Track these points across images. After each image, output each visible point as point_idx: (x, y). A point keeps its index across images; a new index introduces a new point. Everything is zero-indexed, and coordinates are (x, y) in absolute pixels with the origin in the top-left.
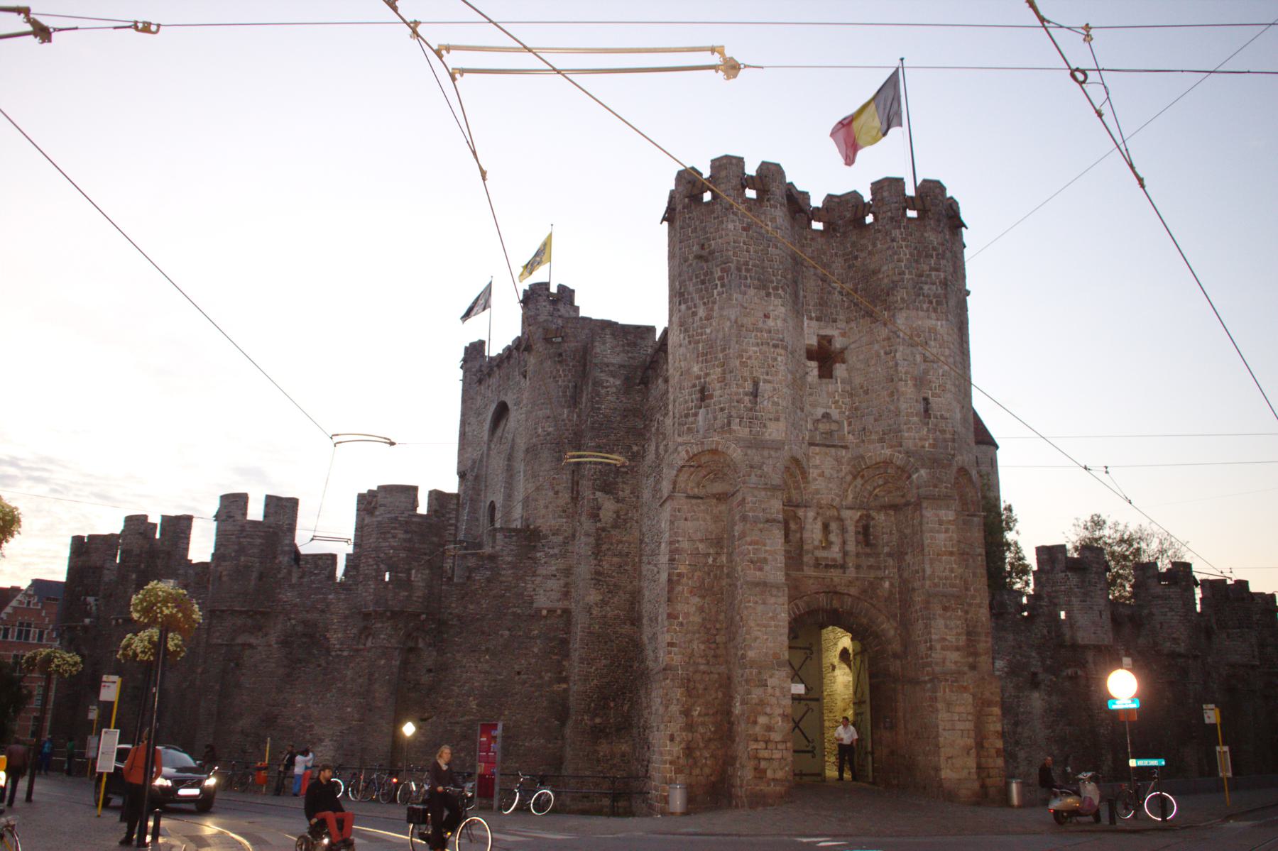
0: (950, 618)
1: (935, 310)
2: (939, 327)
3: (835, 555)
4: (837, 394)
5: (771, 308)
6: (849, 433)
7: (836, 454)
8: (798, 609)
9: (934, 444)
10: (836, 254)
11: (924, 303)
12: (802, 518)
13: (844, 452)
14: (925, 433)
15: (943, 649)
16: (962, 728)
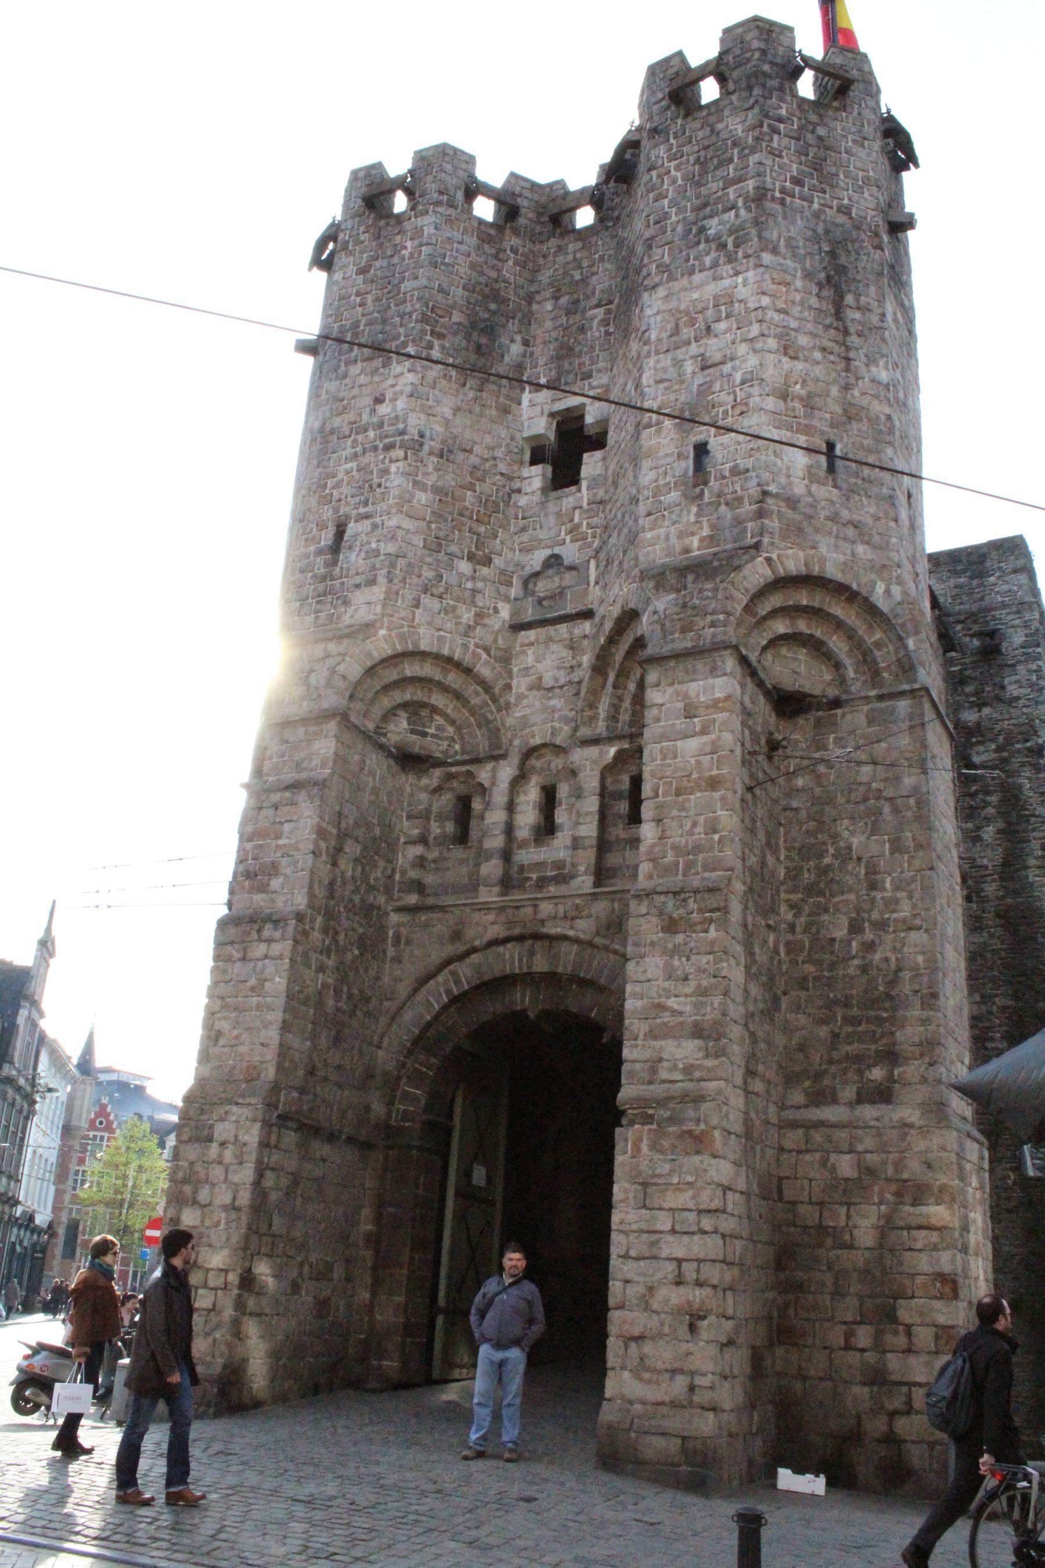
0: (676, 951)
1: (731, 259)
2: (740, 286)
3: (562, 855)
4: (577, 513)
5: (390, 382)
6: (597, 583)
7: (571, 633)
8: (457, 982)
9: (711, 537)
10: (602, 259)
11: (707, 254)
12: (486, 784)
13: (587, 627)
14: (692, 519)
15: (652, 1035)
16: (680, 1253)
